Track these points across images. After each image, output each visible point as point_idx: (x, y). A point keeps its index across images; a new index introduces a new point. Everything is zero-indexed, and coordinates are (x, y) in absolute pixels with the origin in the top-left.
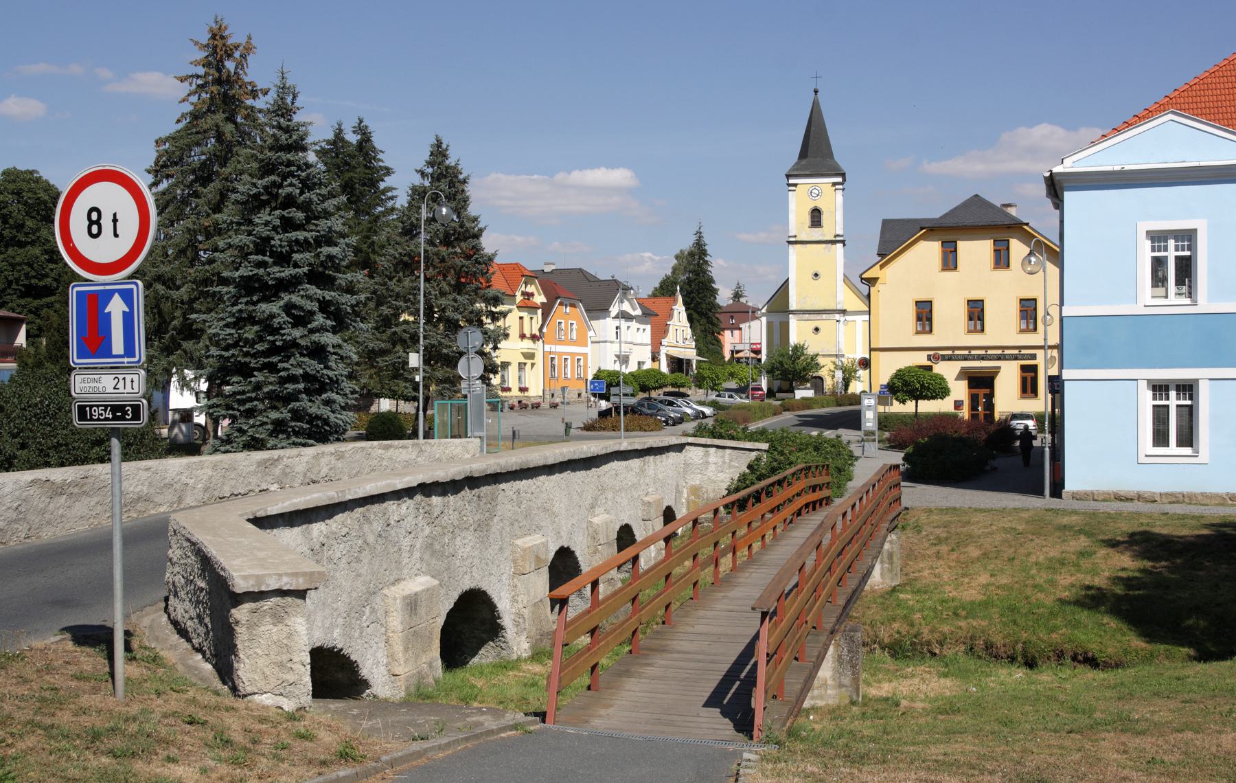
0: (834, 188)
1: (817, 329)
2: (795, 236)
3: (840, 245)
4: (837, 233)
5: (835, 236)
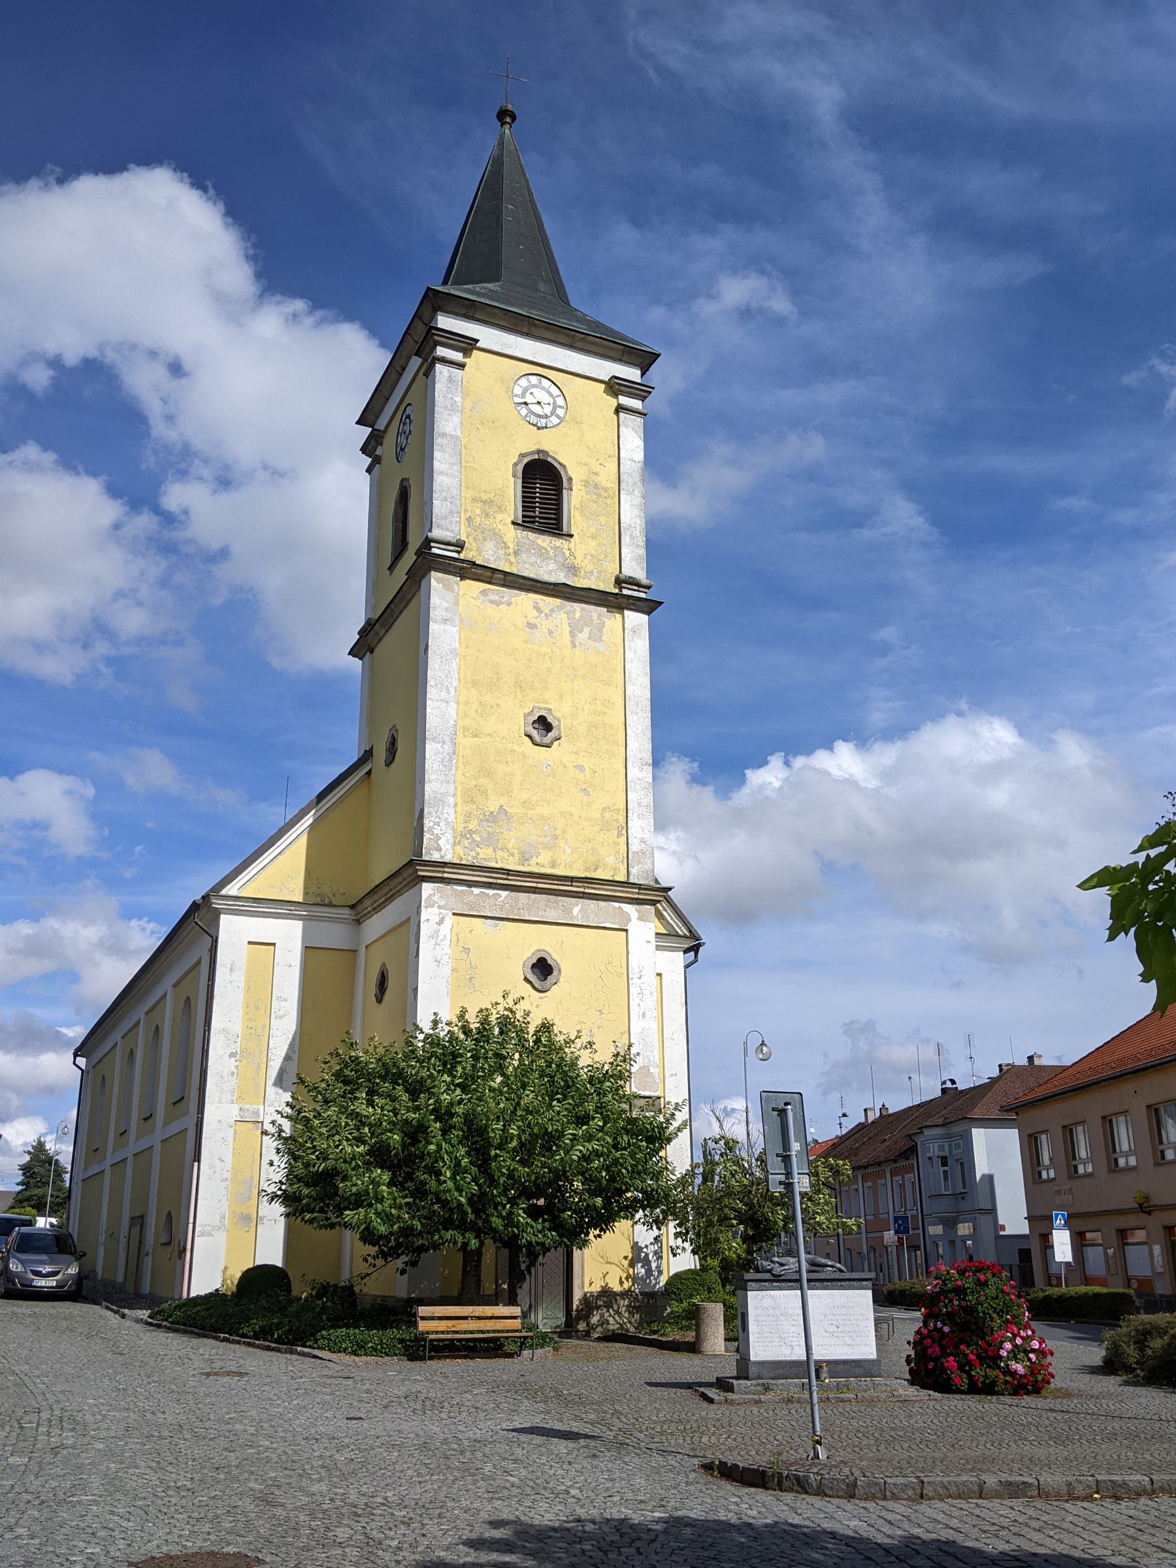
0: (613, 402)
1: (543, 968)
2: (460, 545)
3: (636, 620)
4: (628, 571)
5: (619, 582)
